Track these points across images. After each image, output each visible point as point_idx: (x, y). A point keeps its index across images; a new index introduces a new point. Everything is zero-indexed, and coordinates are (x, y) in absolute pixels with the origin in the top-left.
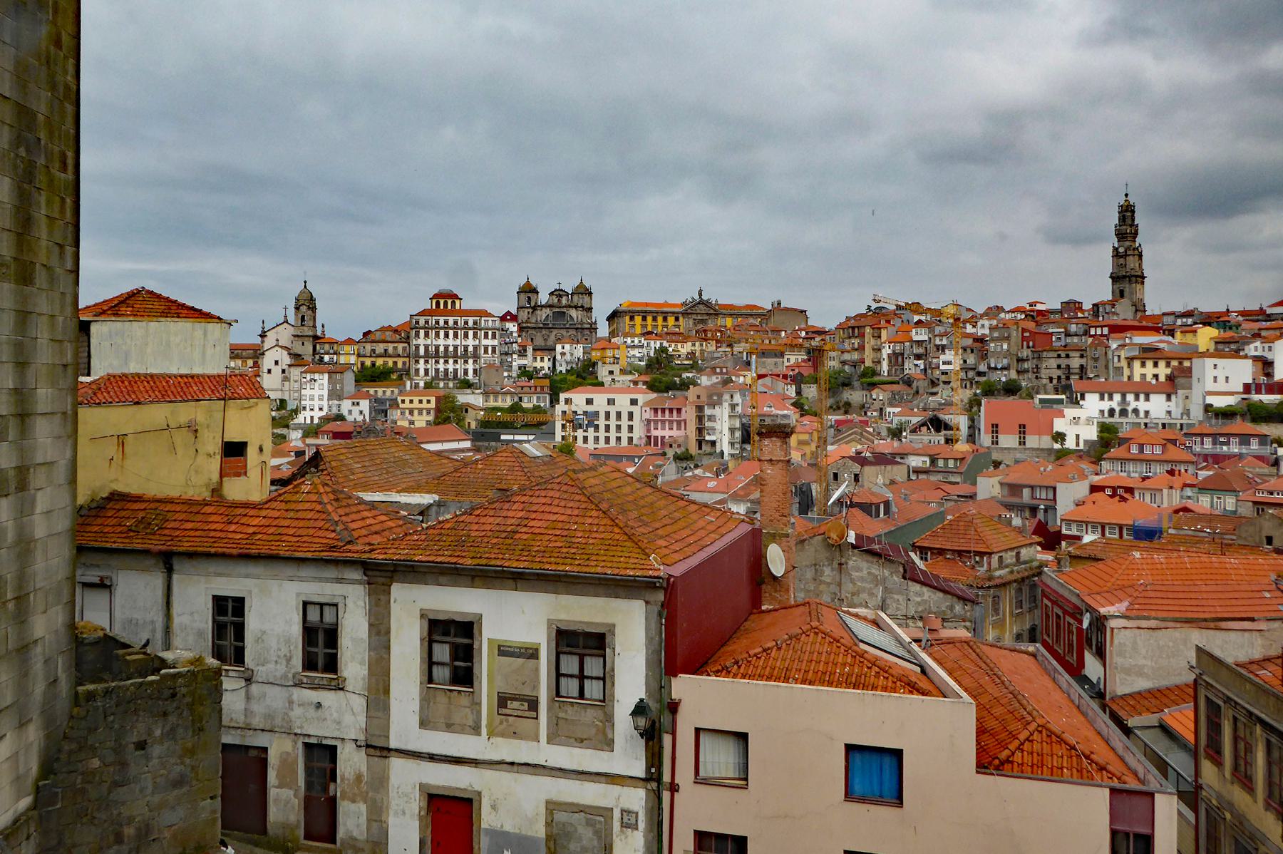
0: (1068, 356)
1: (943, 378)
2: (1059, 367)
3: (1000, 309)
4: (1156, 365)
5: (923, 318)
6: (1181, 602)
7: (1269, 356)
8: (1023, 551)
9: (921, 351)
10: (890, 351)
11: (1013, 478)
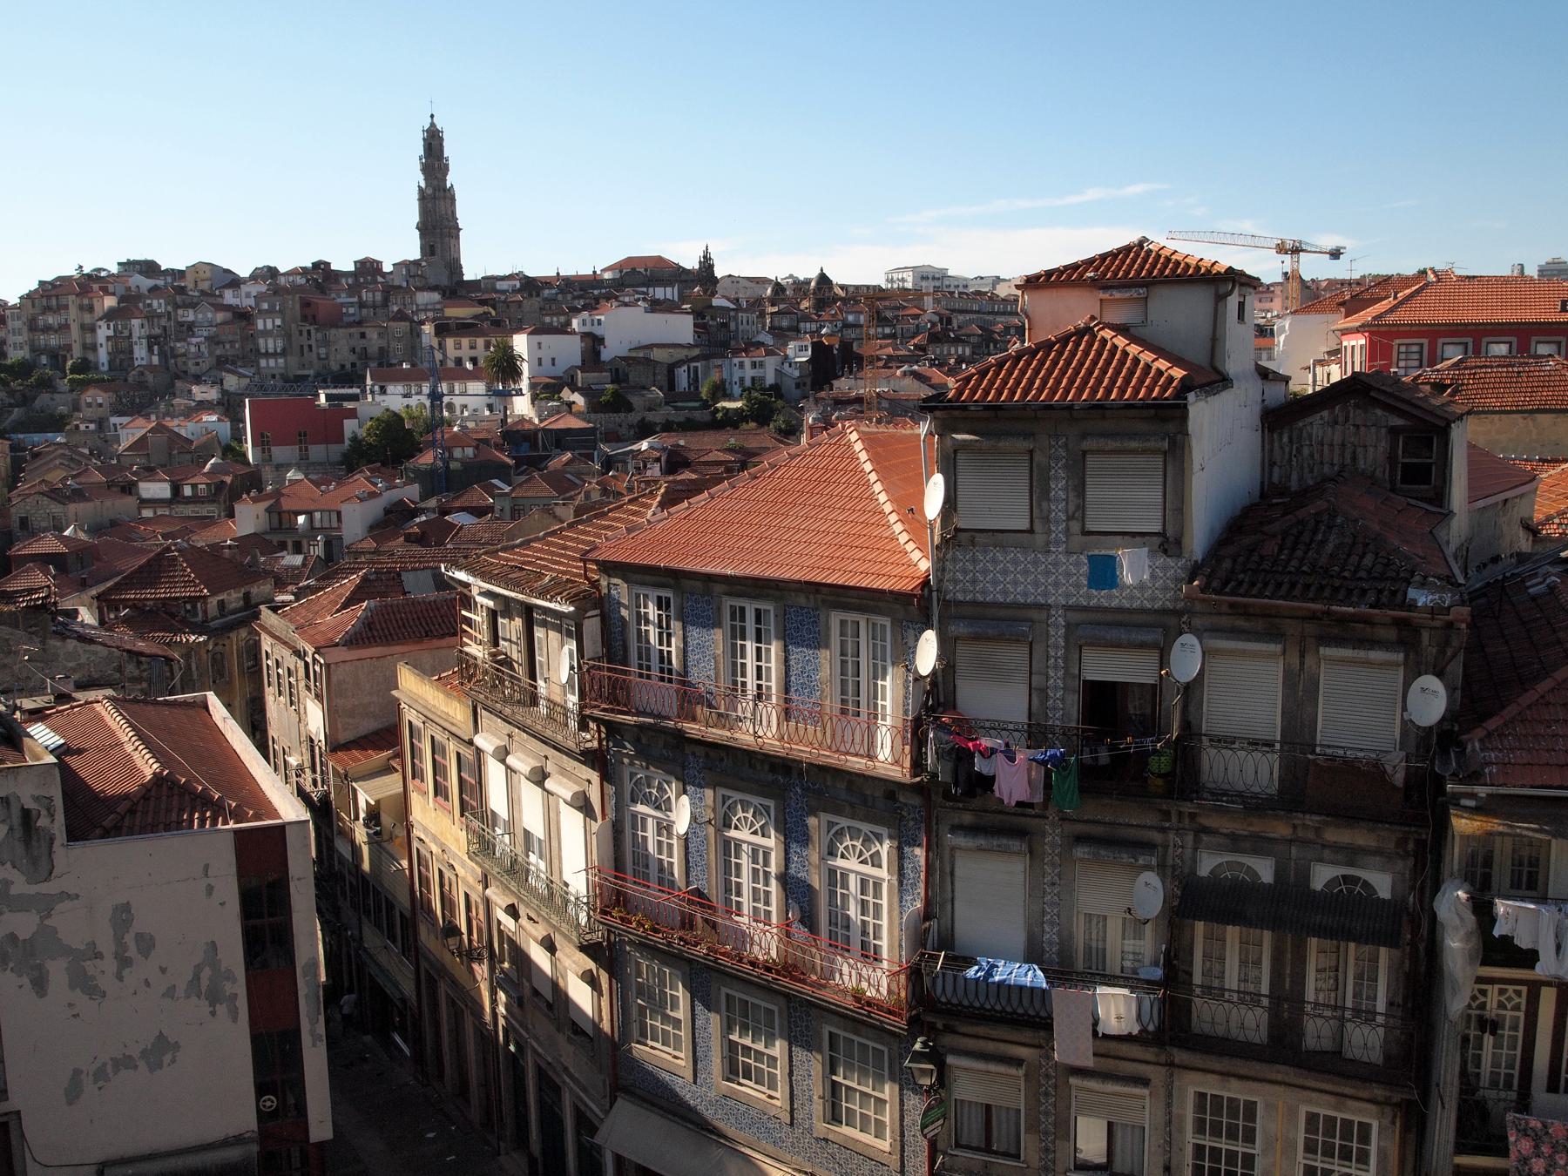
0: (363, 335)
2: (353, 350)
3: (272, 272)
5: (160, 283)
7: (598, 331)
9: (157, 331)
10: (111, 333)
11: (287, 505)
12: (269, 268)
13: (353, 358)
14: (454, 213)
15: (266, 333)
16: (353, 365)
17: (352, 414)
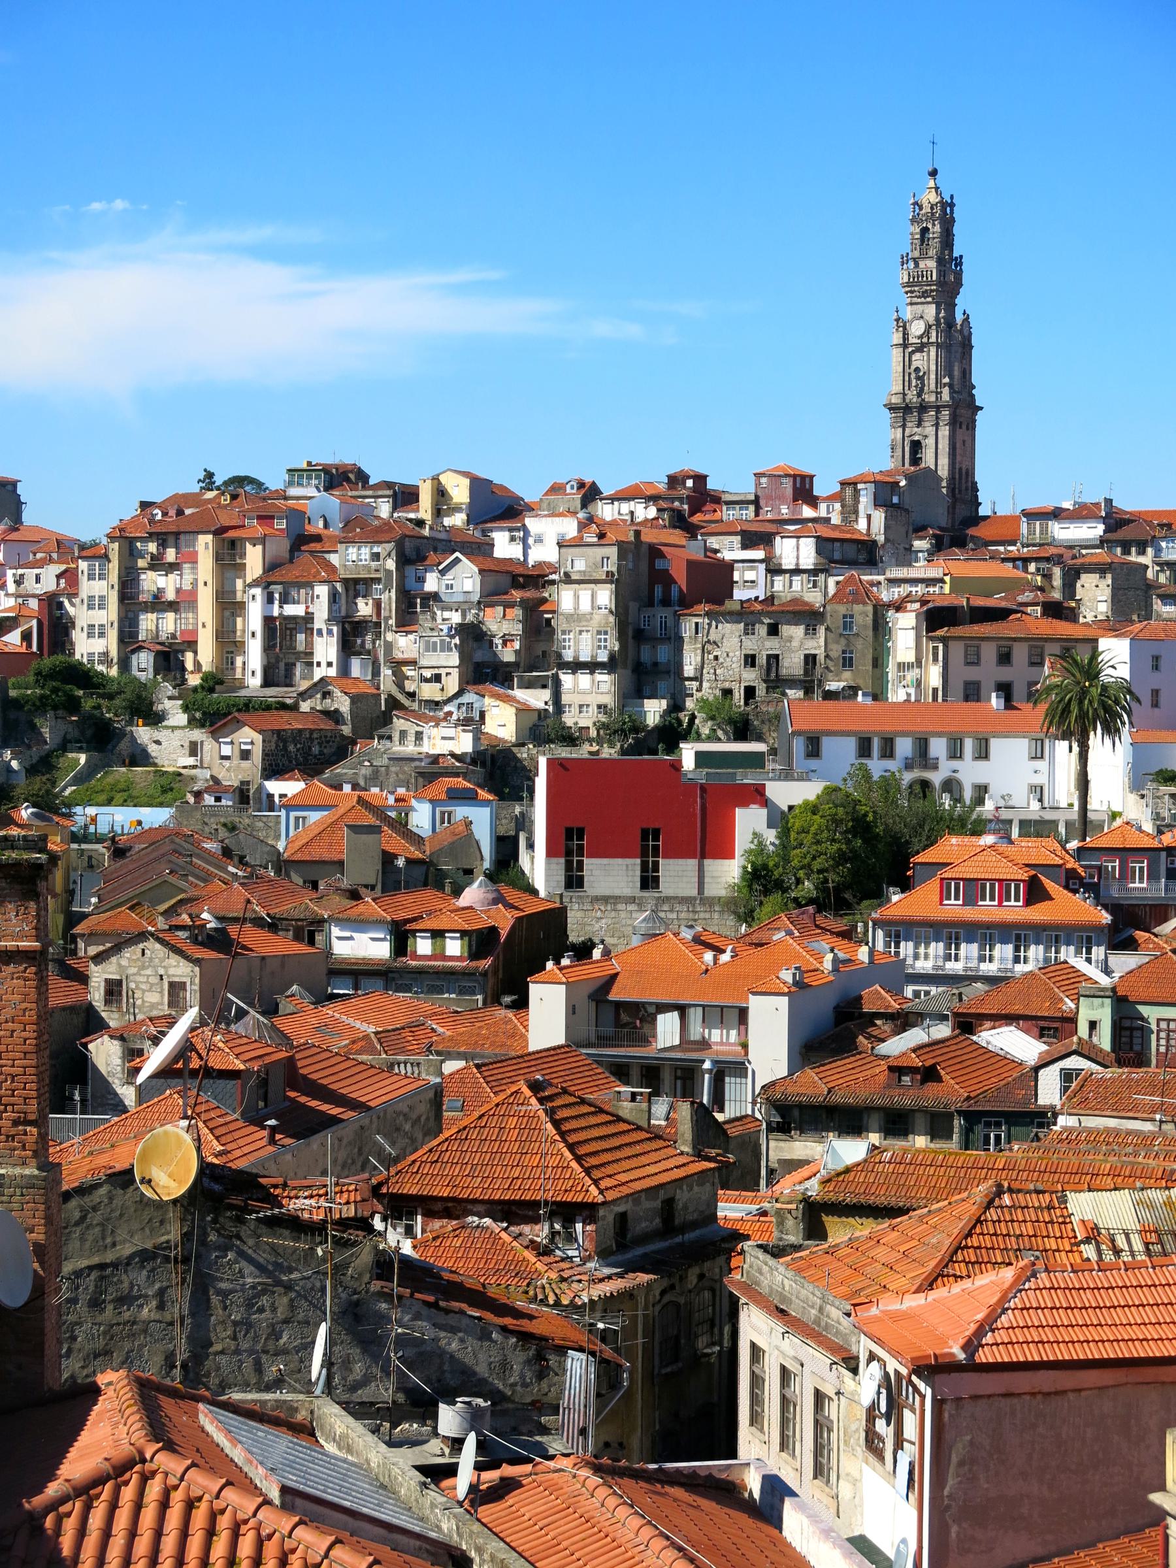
0: (773, 630)
1: (429, 691)
2: (750, 660)
3: (590, 494)
4: (1005, 658)
6: (1119, 1316)
8: (682, 1196)
9: (364, 608)
12: (581, 485)
13: (751, 677)
14: (966, 374)
15: (576, 617)
16: (750, 692)
17: (757, 795)
